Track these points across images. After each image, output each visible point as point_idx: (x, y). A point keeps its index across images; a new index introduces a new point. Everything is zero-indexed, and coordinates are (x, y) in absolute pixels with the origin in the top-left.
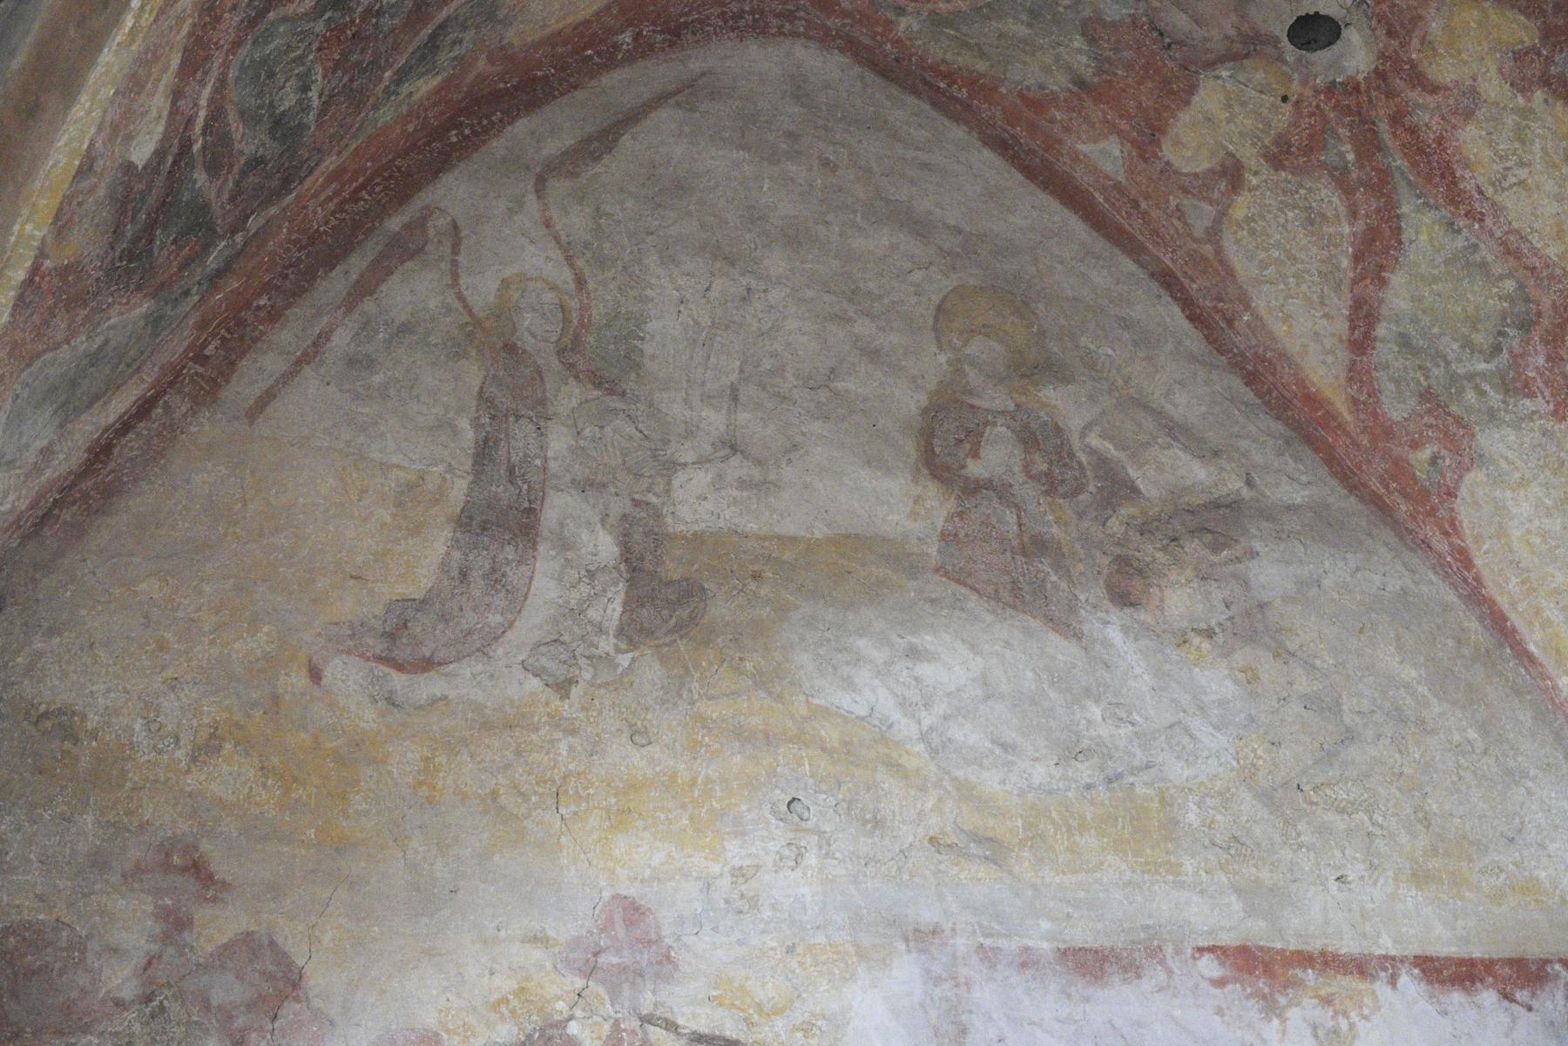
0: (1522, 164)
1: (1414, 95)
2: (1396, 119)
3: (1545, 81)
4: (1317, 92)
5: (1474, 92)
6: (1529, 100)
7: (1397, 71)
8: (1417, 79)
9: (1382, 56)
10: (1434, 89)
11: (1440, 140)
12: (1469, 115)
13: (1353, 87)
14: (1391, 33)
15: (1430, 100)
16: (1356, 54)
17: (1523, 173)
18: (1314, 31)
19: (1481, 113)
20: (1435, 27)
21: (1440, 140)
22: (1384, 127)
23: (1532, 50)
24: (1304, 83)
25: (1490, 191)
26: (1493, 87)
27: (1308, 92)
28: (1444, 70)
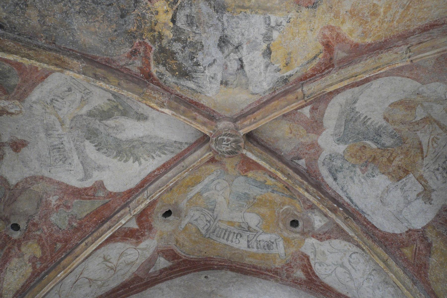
0: (17, 270)
1: (16, 248)
2: (9, 248)
3: (33, 263)
4: (5, 234)
5: (24, 255)
6: (28, 263)
7: (18, 243)
8: (19, 247)
9: (19, 239)
10: (19, 250)
11: (11, 257)
12: (19, 257)
13: (10, 239)
14: (24, 238)
15: (17, 250)
16: (16, 235)
17: (15, 272)
18: (16, 227)
19: (21, 259)
20: (30, 243)
21: (11, 257)
22: (7, 247)
23: (37, 258)
24: (5, 231)
25: (8, 270)
26: (26, 257)
27: (4, 233)
28: (23, 249)
